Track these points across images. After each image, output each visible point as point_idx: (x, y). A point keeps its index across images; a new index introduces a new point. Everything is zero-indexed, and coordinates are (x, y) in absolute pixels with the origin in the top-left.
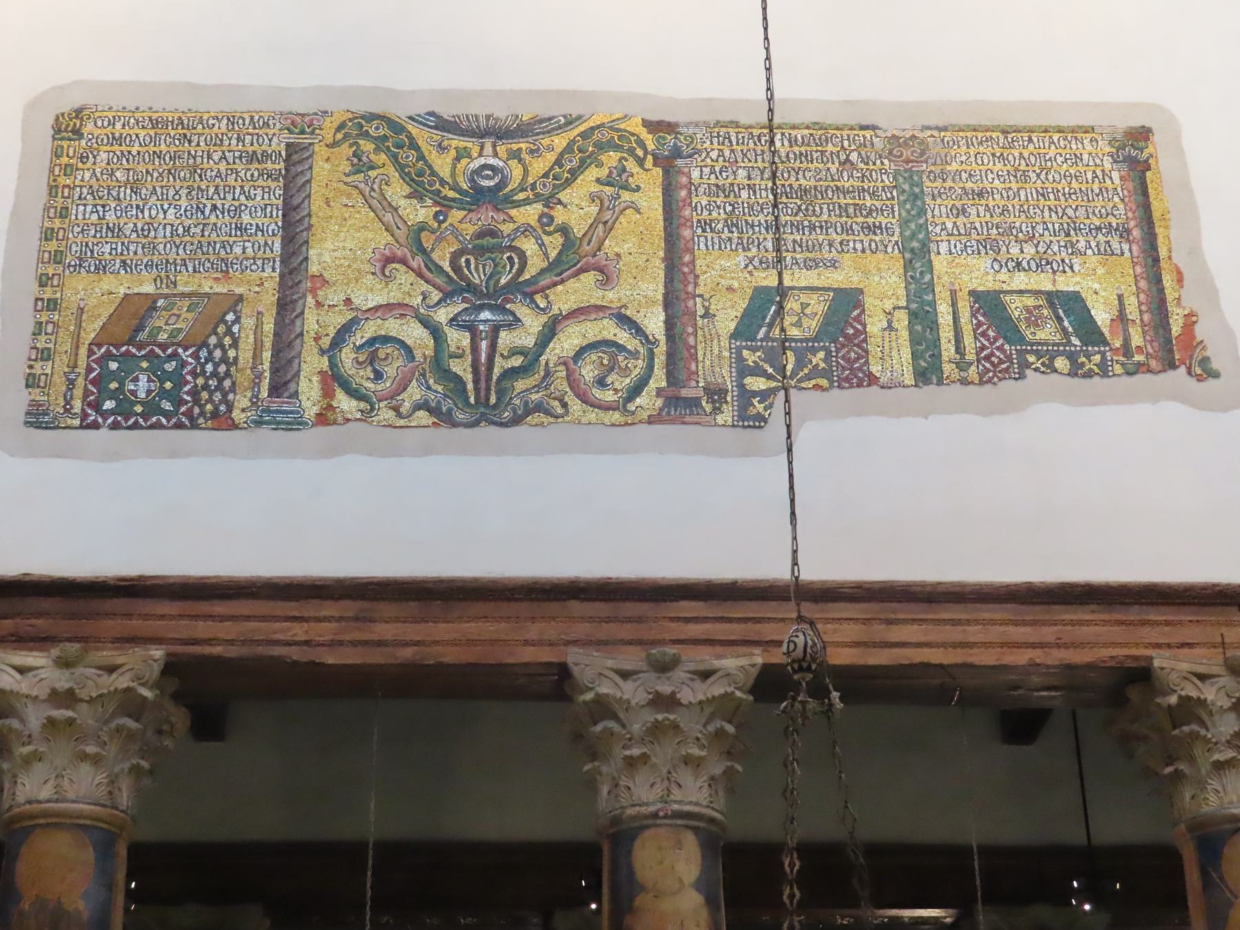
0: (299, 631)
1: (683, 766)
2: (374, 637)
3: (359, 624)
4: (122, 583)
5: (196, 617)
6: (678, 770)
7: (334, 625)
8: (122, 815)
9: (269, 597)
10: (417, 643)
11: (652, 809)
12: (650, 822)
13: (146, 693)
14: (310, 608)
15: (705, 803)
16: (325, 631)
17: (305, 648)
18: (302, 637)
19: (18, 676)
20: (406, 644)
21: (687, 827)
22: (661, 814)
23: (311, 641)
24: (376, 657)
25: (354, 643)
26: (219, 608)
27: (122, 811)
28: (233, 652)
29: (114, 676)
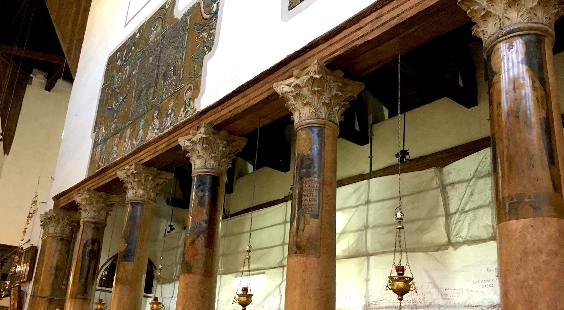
0: (360, 33)
1: (509, 9)
2: (383, 22)
3: (378, 20)
4: (309, 45)
5: (330, 45)
6: (507, 12)
7: (371, 24)
8: (323, 120)
9: (350, 26)
10: (397, 16)
11: (496, 35)
12: (496, 41)
13: (317, 76)
14: (362, 23)
15: (525, 21)
16: (368, 28)
17: (363, 38)
18: (361, 35)
19: (288, 87)
20: (394, 18)
21: (515, 36)
22: (500, 36)
23: (363, 35)
24: (385, 29)
25: (378, 27)
26: (337, 38)
27: (323, 119)
28: (341, 52)
29: (309, 75)
